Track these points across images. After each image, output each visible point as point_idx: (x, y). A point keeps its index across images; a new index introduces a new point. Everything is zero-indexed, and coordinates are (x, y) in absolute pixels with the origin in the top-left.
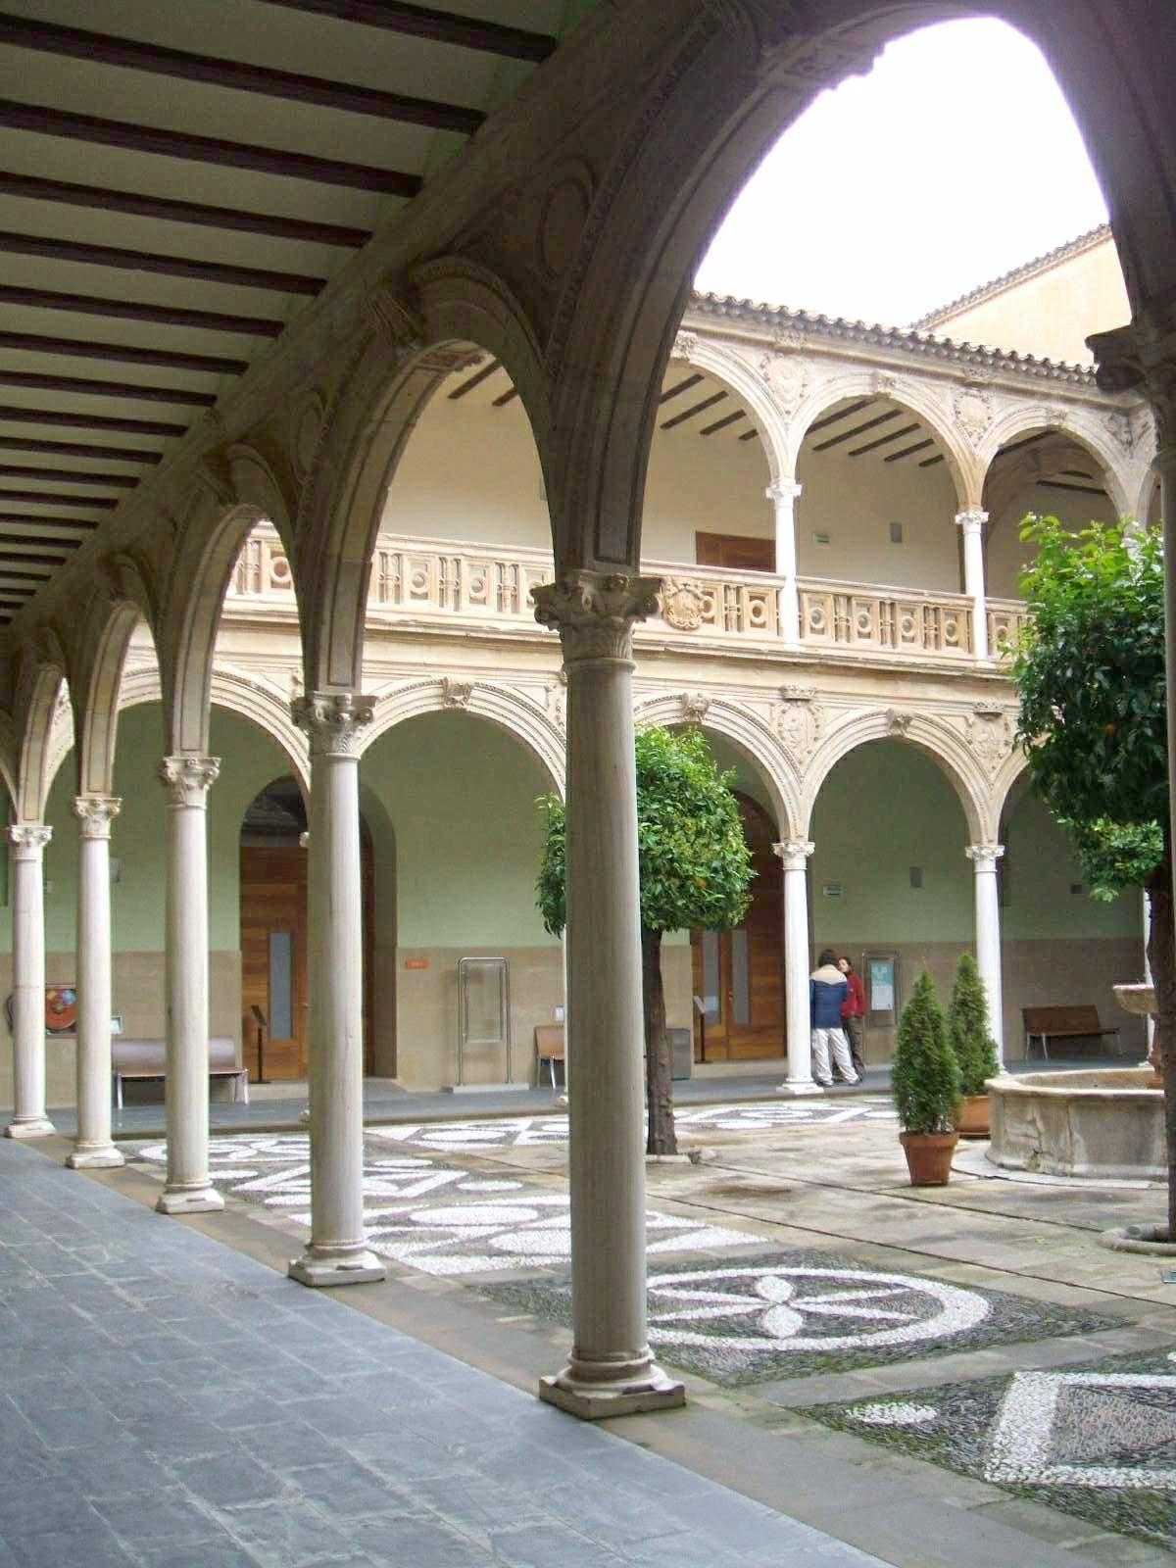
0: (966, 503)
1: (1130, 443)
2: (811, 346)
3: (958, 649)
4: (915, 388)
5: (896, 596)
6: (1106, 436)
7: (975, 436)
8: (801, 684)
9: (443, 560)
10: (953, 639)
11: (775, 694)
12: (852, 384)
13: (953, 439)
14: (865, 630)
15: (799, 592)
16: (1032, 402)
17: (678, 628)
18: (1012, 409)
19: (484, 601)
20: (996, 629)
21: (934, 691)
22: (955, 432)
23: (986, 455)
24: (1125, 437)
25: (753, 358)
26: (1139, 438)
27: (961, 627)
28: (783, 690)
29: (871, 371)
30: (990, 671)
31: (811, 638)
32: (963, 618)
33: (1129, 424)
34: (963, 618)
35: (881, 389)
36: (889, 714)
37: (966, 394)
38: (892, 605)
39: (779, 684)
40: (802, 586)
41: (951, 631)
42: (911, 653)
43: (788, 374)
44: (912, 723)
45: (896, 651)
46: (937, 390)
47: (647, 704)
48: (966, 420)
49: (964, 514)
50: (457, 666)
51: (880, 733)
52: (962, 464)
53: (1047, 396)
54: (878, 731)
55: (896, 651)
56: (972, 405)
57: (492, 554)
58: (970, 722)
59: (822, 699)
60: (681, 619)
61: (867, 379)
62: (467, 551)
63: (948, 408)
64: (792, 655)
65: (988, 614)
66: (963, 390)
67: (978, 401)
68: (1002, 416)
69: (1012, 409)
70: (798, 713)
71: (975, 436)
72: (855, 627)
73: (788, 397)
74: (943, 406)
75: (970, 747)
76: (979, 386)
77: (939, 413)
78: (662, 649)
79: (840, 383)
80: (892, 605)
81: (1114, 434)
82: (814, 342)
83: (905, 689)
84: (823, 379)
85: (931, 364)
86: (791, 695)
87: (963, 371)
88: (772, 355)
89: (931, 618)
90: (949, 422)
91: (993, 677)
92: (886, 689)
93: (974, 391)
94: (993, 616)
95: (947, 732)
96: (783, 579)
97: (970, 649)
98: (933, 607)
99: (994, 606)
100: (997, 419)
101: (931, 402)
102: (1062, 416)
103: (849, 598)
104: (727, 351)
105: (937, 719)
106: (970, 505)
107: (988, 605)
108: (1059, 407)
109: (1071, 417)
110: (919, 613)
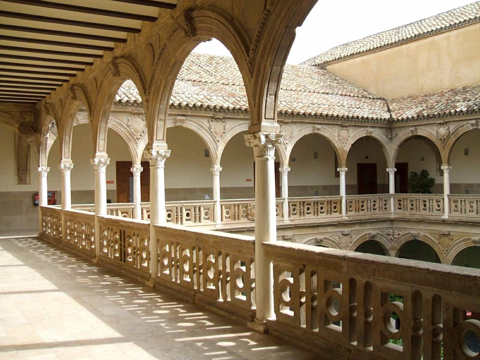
0: (341, 165)
1: (391, 138)
2: (294, 121)
3: (337, 213)
4: (326, 129)
5: (319, 199)
6: (384, 137)
7: (345, 143)
10: (335, 210)
12: (306, 130)
13: (337, 144)
14: (309, 212)
15: (289, 202)
16: (363, 129)
17: (251, 220)
18: (356, 132)
20: (349, 205)
21: (329, 229)
22: (338, 143)
23: (347, 148)
24: (390, 137)
26: (394, 137)
27: (338, 206)
28: (283, 236)
29: (313, 125)
30: (347, 221)
31: (293, 217)
32: (339, 203)
33: (391, 133)
34: (339, 203)
35: (316, 132)
36: (316, 239)
37: (342, 129)
38: (317, 202)
39: (282, 235)
40: (289, 201)
41: (335, 207)
42: (323, 218)
45: (318, 217)
46: (333, 129)
48: (342, 138)
49: (340, 169)
52: (340, 152)
53: (367, 127)
55: (318, 217)
57: (192, 204)
58: (340, 237)
59: (296, 238)
60: (252, 217)
61: (312, 128)
62: (184, 205)
63: (336, 135)
64: (287, 225)
65: (346, 201)
66: (341, 128)
67: (345, 131)
68: (353, 135)
69: (356, 132)
71: (345, 143)
72: (306, 211)
74: (335, 134)
75: (340, 245)
76: (346, 126)
77: (334, 137)
78: (247, 229)
79: (303, 131)
80: (317, 202)
81: (387, 136)
82: (296, 119)
83: (321, 230)
84: (298, 130)
86: (286, 238)
87: (341, 122)
88: (282, 124)
89: (329, 205)
90: (337, 139)
91: (348, 222)
92: (315, 231)
93: (345, 128)
94: (348, 201)
95: (333, 242)
96: (284, 199)
97: (341, 213)
98: (329, 201)
99: (348, 198)
100: (351, 136)
101: (330, 133)
102: (371, 133)
105: (331, 238)
106: (342, 166)
107: (347, 198)
108: (370, 130)
109: (374, 132)
110: (326, 204)
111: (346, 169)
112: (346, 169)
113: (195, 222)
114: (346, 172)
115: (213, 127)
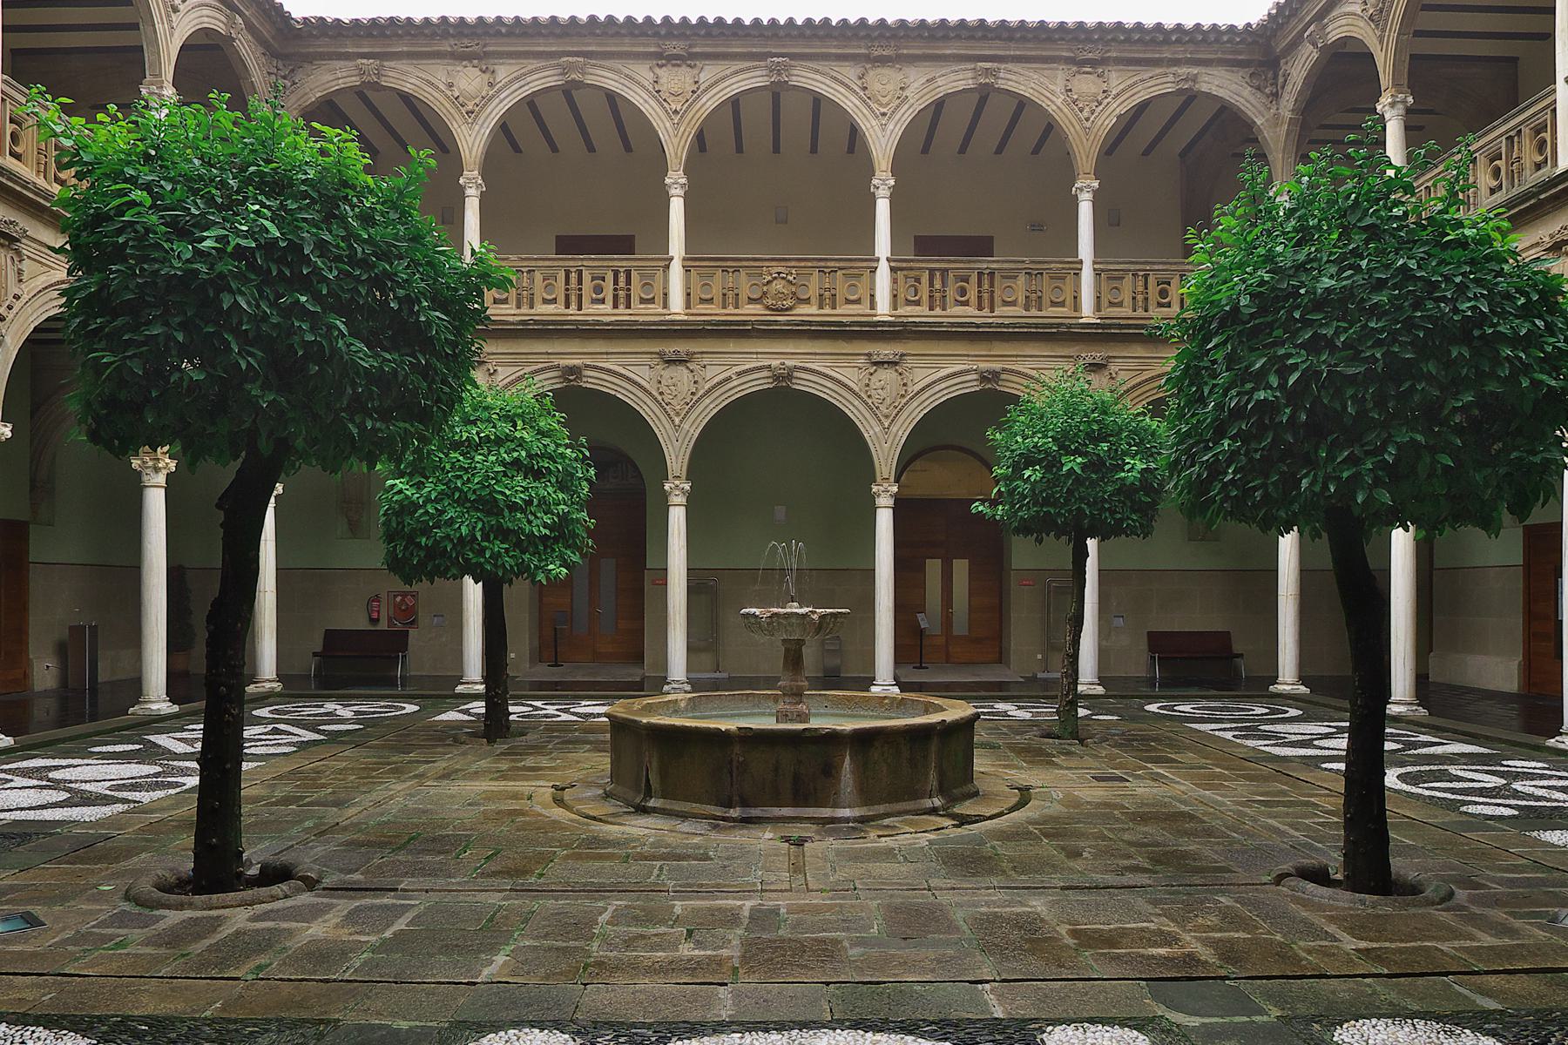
6: (1247, 92)
8: (886, 351)
9: (568, 273)
11: (862, 359)
12: (955, 80)
19: (603, 301)
25: (850, 72)
28: (869, 355)
43: (884, 80)
44: (1003, 376)
46: (1046, 73)
47: (739, 374)
50: (571, 354)
51: (975, 387)
53: (1176, 62)
54: (971, 385)
56: (1086, 85)
63: (1058, 88)
70: (886, 375)
73: (884, 101)
76: (1094, 63)
81: (1258, 88)
85: (1031, 49)
86: (875, 358)
90: (1059, 102)
102: (1194, 79)
103: (947, 270)
104: (827, 70)
105: (1034, 373)
111: (1096, 184)
112: (1096, 184)
113: (519, 307)
114: (1096, 193)
115: (663, 80)
